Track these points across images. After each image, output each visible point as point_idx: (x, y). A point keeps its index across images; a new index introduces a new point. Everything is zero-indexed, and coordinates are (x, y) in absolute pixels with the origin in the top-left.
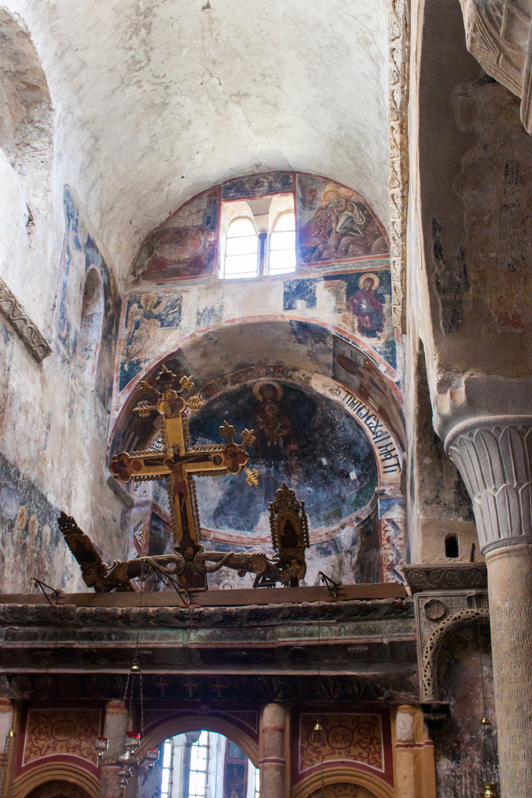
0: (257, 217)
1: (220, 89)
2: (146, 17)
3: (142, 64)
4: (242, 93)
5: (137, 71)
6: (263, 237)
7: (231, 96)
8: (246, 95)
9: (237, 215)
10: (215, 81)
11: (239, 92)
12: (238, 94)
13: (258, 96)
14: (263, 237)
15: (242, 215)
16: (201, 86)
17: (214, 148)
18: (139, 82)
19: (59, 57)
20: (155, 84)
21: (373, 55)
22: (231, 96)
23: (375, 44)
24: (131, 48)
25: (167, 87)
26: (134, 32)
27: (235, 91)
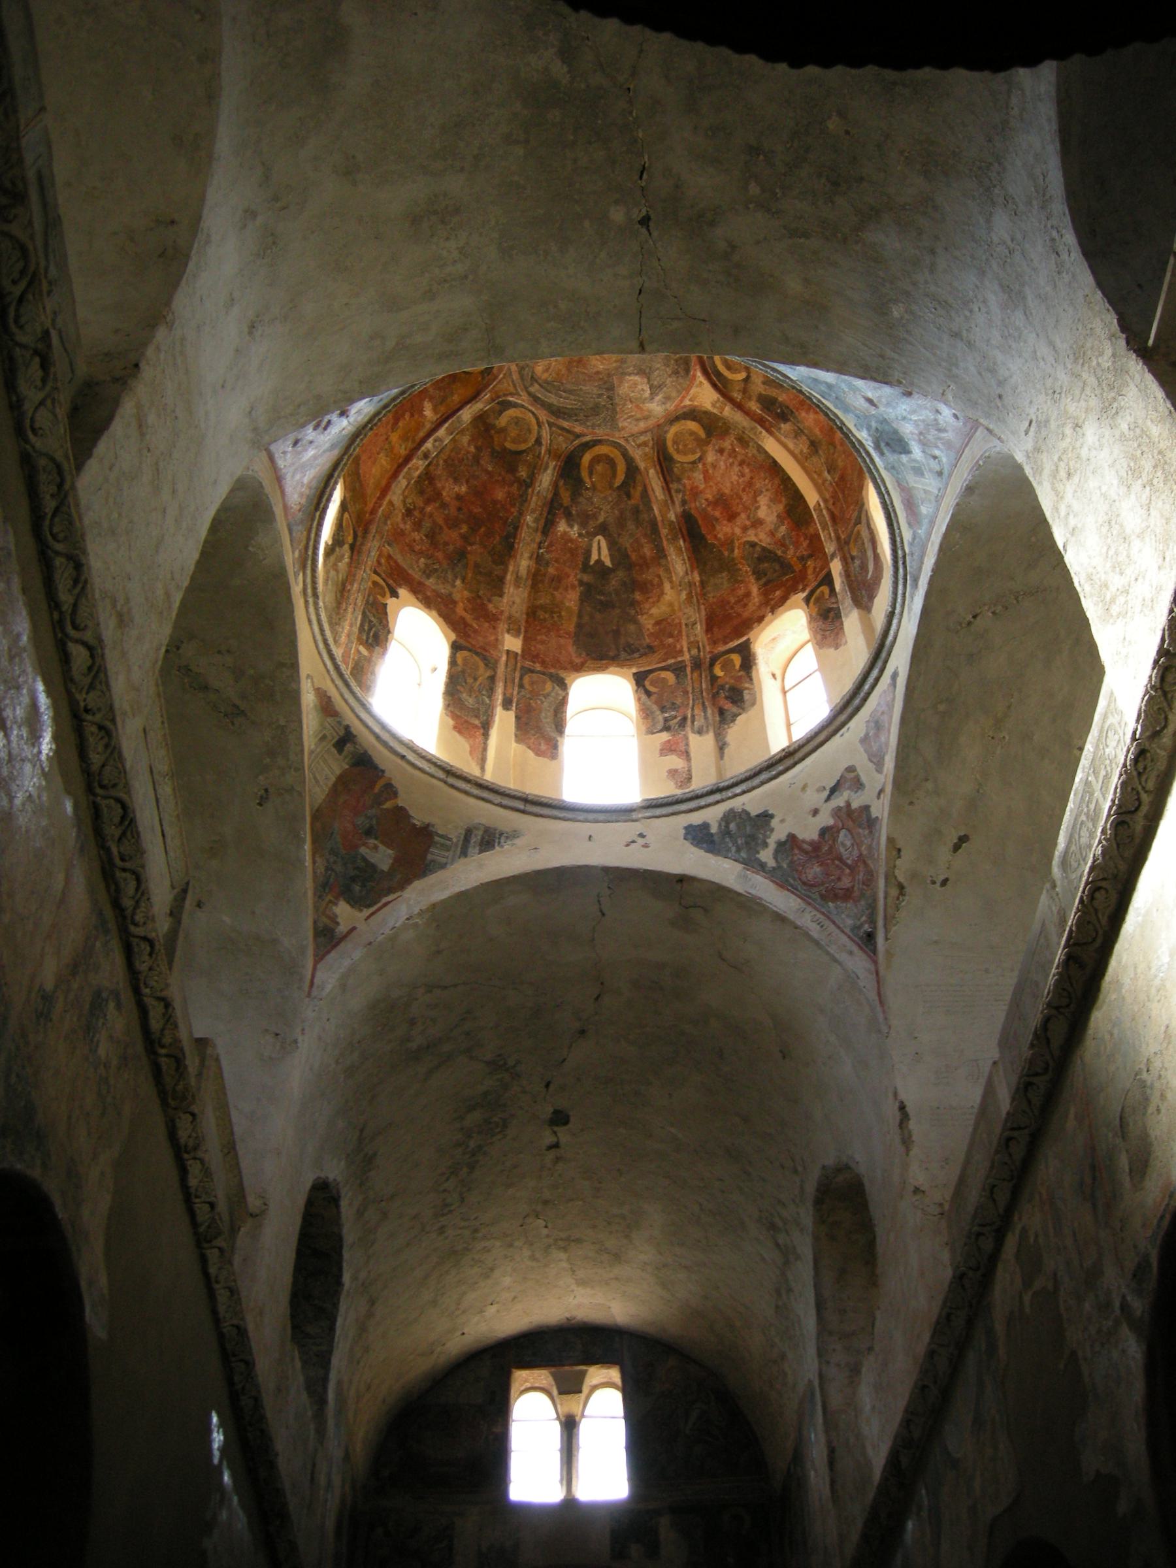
0: (564, 1397)
1: (545, 1231)
2: (473, 1155)
3: (452, 1208)
4: (572, 1238)
5: (443, 1215)
6: (570, 1425)
7: (556, 1240)
8: (578, 1241)
9: (528, 1385)
10: (541, 1223)
11: (570, 1236)
12: (568, 1239)
13: (594, 1243)
14: (570, 1425)
15: (537, 1385)
16: (520, 1228)
17: (515, 1298)
18: (443, 1227)
19: (360, 1213)
20: (460, 1228)
21: (781, 1241)
22: (556, 1240)
23: (787, 1232)
24: (445, 1191)
25: (476, 1231)
26: (452, 1173)
27: (563, 1235)
